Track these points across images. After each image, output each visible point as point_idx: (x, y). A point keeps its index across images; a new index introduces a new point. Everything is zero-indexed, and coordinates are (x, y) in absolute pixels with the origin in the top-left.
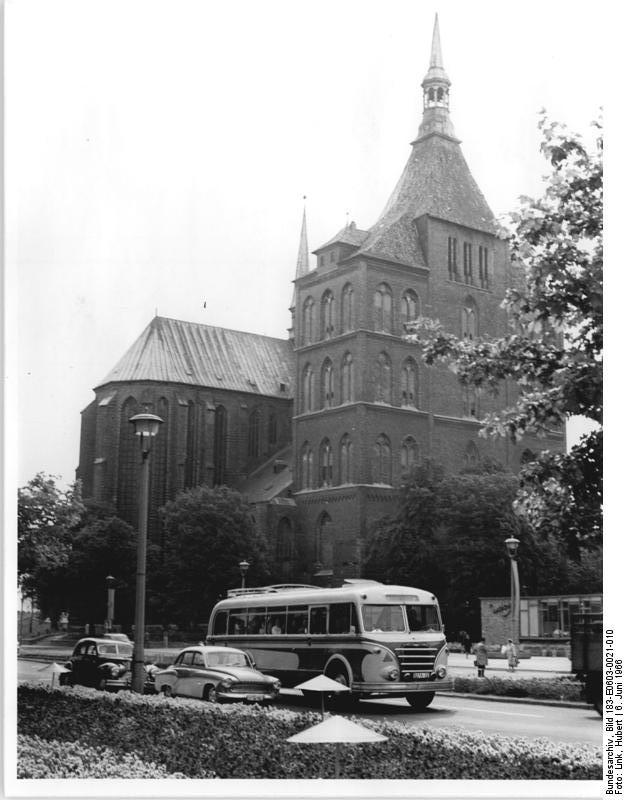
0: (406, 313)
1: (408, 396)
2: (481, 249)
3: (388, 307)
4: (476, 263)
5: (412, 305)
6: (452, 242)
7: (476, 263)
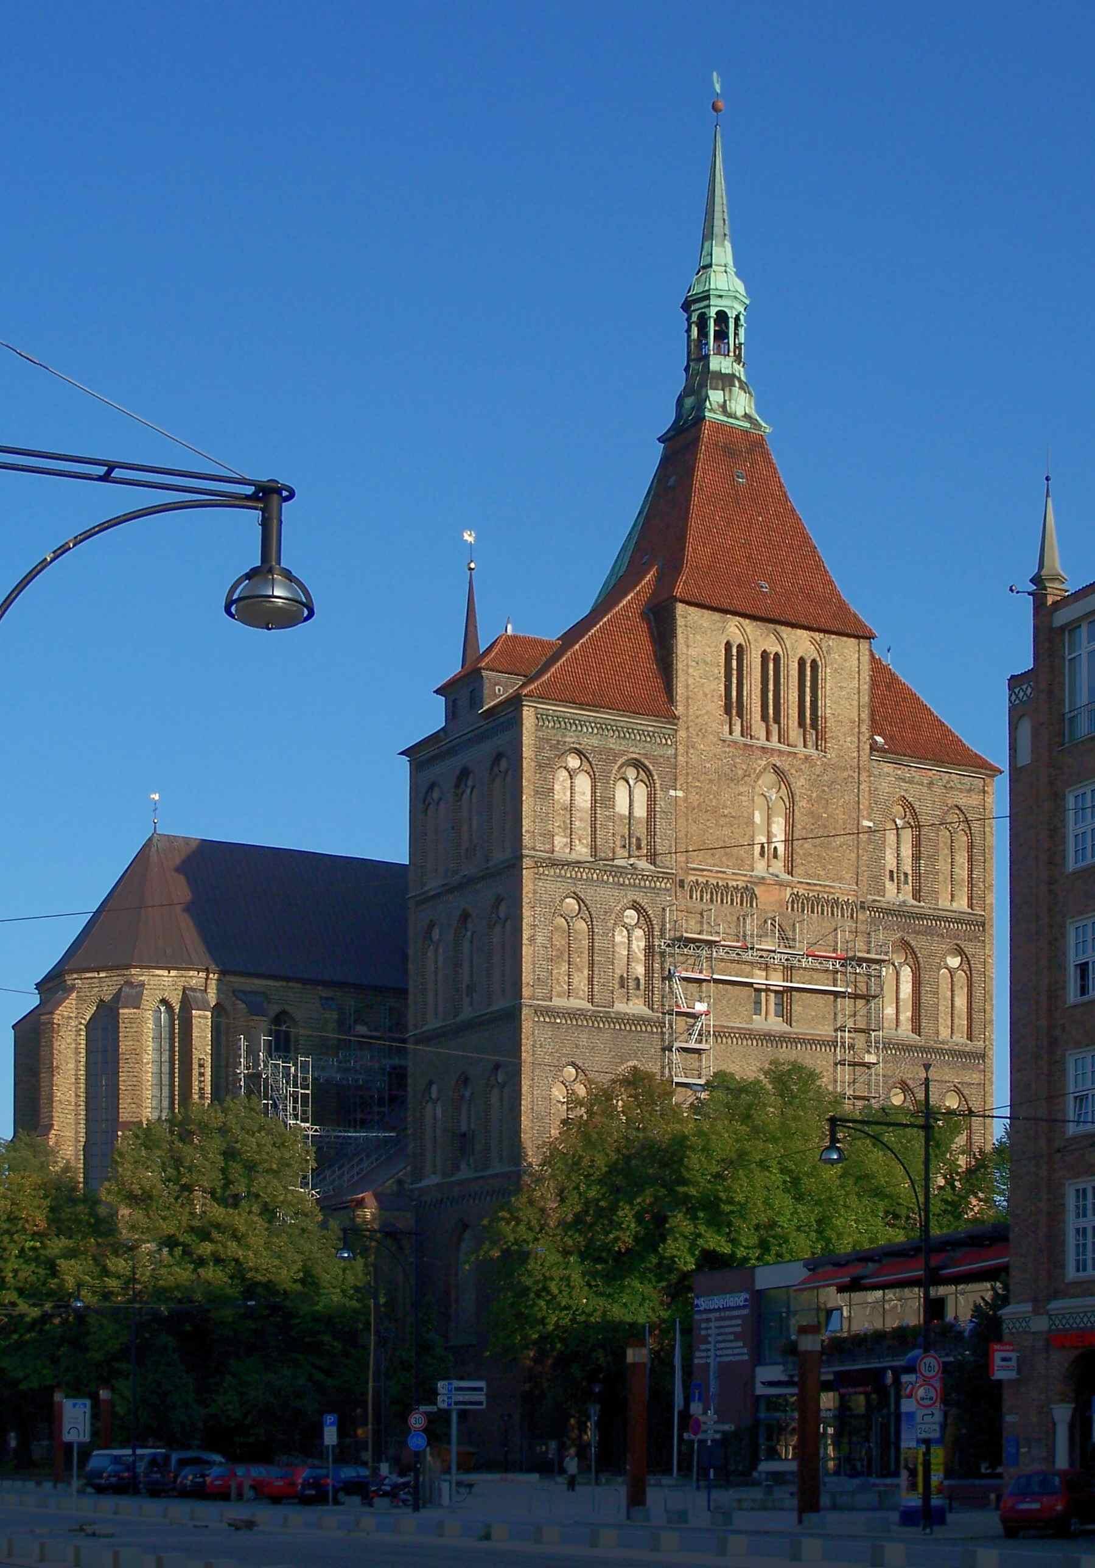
1: (632, 984)
2: (802, 662)
3: (584, 800)
4: (791, 696)
5: (641, 792)
7: (791, 696)
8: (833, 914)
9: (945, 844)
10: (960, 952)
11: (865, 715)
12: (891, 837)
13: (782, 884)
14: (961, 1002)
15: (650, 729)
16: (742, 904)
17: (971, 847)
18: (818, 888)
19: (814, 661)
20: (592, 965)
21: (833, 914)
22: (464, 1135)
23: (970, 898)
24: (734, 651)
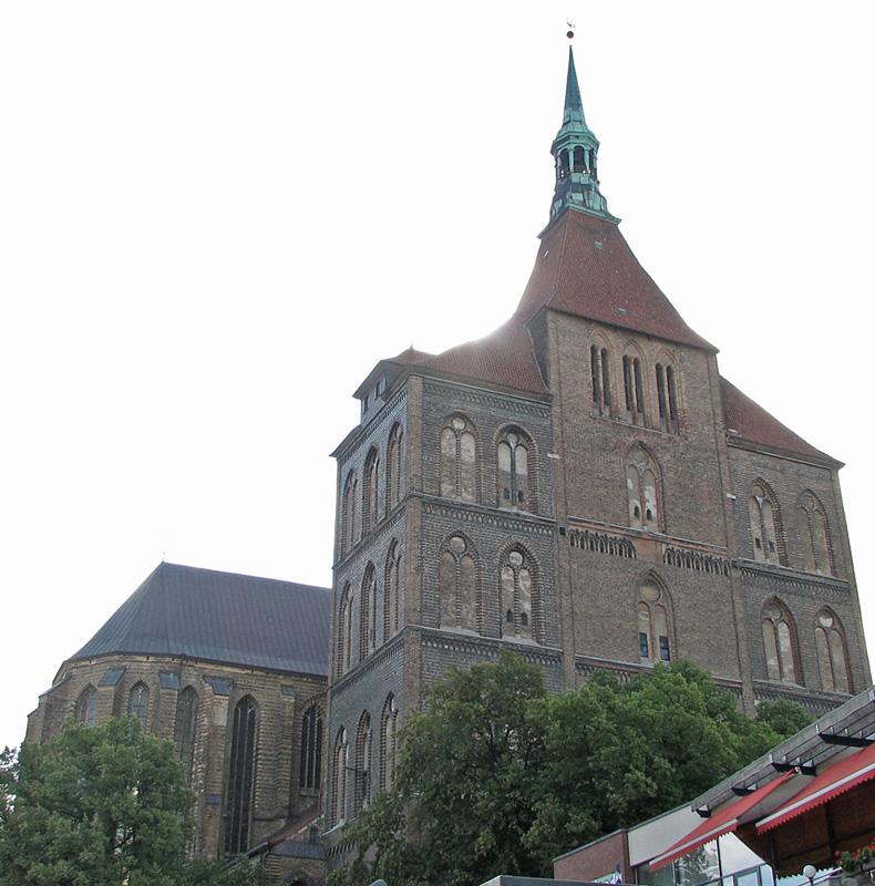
0: (508, 468)
2: (659, 368)
5: (521, 454)
6: (598, 358)
8: (708, 570)
9: (803, 520)
10: (829, 612)
11: (718, 411)
12: (754, 512)
13: (656, 540)
14: (838, 658)
15: (527, 403)
16: (621, 554)
17: (827, 525)
18: (691, 546)
19: (669, 369)
20: (479, 597)
21: (708, 570)
22: (365, 774)
23: (833, 568)
24: (599, 353)
